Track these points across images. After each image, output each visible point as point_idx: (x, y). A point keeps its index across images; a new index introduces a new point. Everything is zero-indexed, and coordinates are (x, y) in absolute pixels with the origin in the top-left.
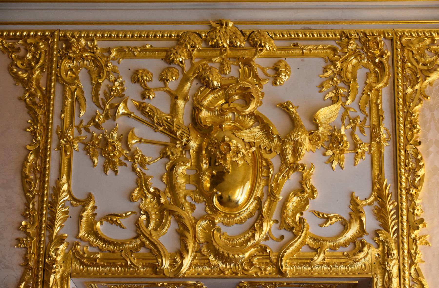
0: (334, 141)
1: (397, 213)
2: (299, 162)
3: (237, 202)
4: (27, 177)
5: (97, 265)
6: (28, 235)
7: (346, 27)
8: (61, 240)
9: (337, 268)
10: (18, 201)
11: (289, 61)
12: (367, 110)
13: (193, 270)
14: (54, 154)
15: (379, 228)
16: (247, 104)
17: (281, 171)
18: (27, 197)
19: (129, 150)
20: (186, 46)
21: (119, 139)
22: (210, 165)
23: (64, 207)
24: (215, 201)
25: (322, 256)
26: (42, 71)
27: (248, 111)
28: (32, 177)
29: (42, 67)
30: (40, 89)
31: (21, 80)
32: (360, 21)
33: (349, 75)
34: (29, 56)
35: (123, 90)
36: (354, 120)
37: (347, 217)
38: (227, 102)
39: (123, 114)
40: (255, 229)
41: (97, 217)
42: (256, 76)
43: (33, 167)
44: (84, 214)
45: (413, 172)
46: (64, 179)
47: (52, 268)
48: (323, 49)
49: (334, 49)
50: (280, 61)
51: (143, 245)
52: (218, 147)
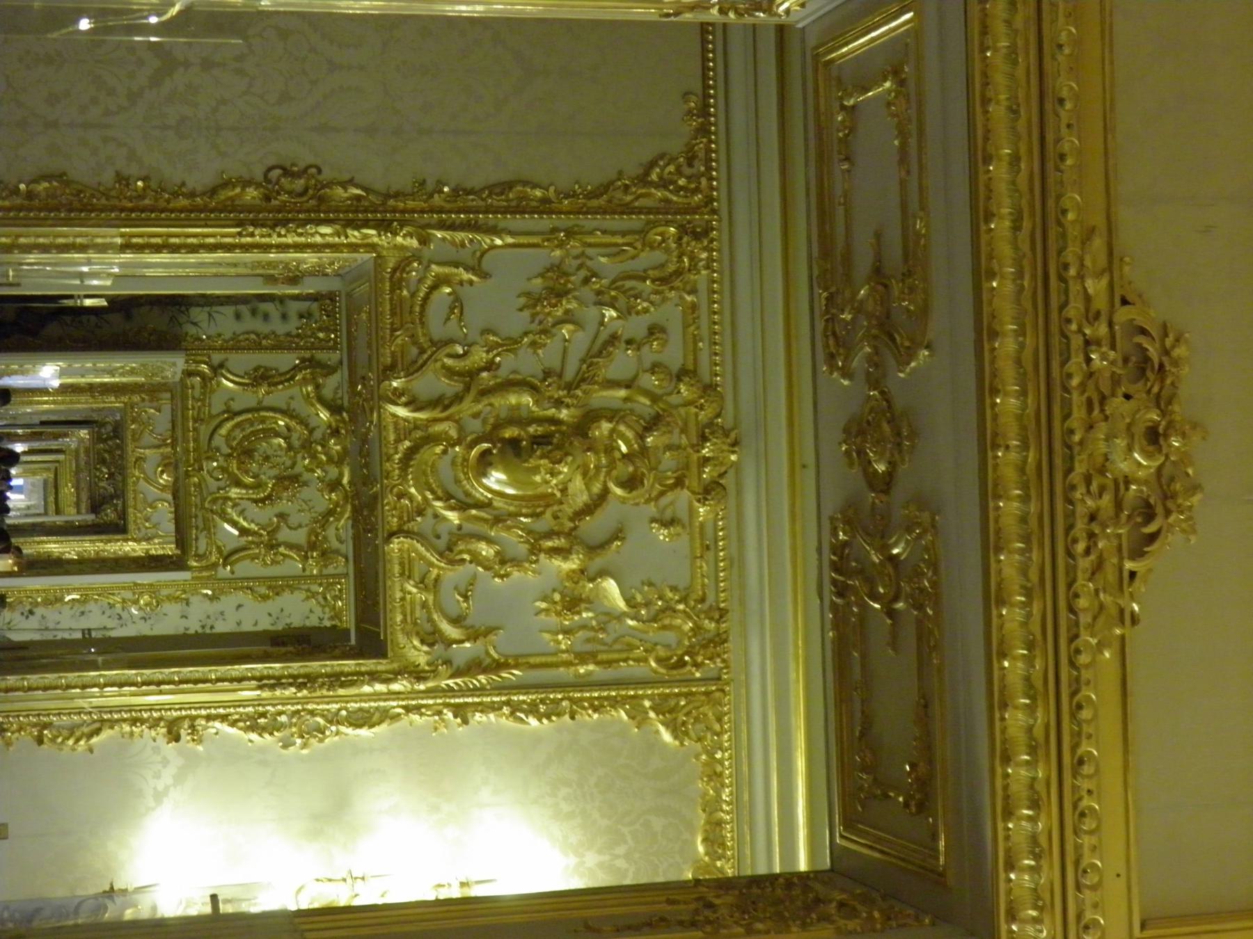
0: (573, 603)
1: (475, 689)
2: (542, 556)
3: (485, 475)
4: (511, 188)
5: (392, 291)
6: (431, 196)
7: (734, 616)
8: (424, 241)
9: (399, 610)
10: (476, 181)
11: (685, 538)
12: (617, 647)
13: (390, 419)
14: (546, 222)
15: (455, 666)
16: (622, 485)
17: (530, 532)
18: (482, 190)
19: (554, 325)
20: (701, 397)
21: (567, 312)
22: (535, 437)
23: (471, 241)
24: (486, 445)
25: (414, 590)
26: (661, 200)
27: (612, 486)
28: (511, 196)
29: (667, 201)
30: (637, 199)
31: (647, 173)
32: (745, 637)
33: (667, 622)
34: (682, 182)
35: (638, 313)
36: (603, 630)
37: (468, 622)
38: (624, 456)
39: (604, 316)
40: (448, 500)
41: (458, 288)
42: (662, 494)
43: (525, 197)
44: (461, 269)
45: (532, 710)
46: (510, 240)
47: (386, 232)
48: (703, 585)
49: (703, 600)
50: (684, 527)
51: (422, 351)
52: (559, 447)
